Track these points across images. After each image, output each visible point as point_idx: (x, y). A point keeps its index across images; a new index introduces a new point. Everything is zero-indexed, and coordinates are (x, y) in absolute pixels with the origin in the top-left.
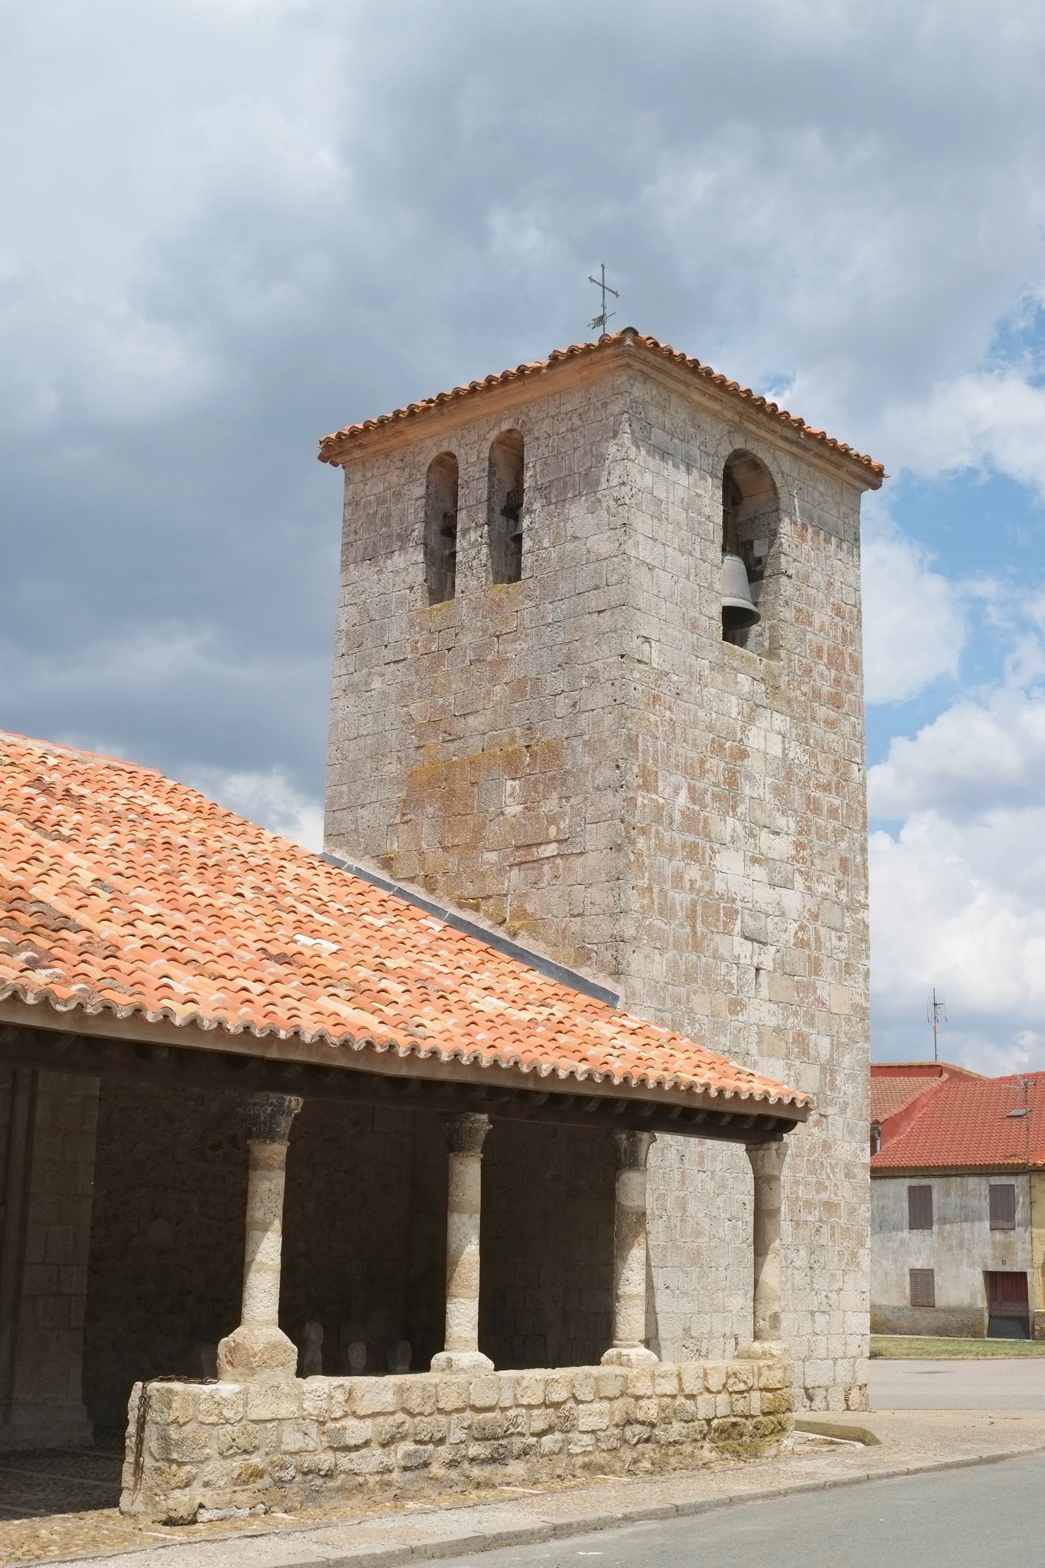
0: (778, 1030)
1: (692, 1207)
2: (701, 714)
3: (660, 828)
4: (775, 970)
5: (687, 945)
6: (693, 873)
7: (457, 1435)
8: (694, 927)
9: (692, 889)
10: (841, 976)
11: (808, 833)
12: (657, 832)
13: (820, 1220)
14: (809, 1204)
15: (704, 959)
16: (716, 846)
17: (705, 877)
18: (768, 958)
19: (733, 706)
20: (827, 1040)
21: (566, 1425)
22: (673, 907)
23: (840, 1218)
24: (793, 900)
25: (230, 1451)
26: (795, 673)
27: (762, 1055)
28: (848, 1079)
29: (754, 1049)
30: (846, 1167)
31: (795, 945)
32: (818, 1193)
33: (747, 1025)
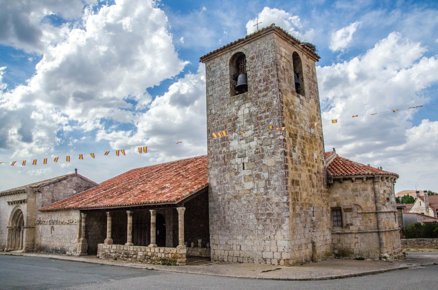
0: (250, 175)
1: (227, 218)
2: (225, 116)
3: (216, 144)
4: (248, 162)
5: (223, 164)
6: (225, 149)
7: (123, 253)
8: (225, 160)
9: (224, 153)
10: (271, 156)
11: (258, 125)
12: (215, 145)
13: (266, 218)
14: (262, 214)
15: (227, 166)
16: (230, 141)
17: (227, 149)
18: (246, 160)
19: (234, 109)
20: (267, 174)
21: (137, 254)
22: (219, 158)
23: (274, 217)
24: (253, 144)
25: (101, 251)
26: (252, 91)
27: (245, 182)
28: (276, 181)
29: (243, 181)
30: (276, 203)
31: (255, 154)
32: (265, 211)
33: (241, 177)
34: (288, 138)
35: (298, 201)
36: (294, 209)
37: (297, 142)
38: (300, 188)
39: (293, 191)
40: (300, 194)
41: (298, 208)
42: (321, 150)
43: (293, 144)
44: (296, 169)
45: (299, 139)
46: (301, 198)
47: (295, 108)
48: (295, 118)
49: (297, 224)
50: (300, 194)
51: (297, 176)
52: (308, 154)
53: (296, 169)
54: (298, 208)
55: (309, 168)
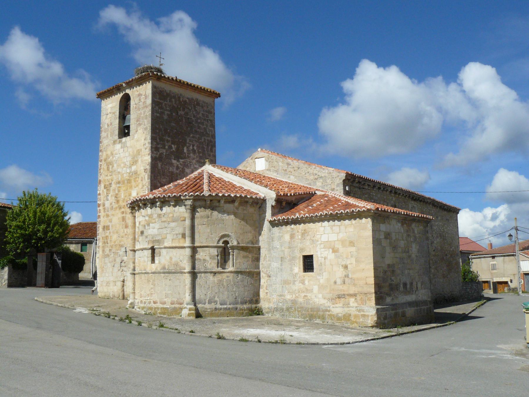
34: (103, 191)
35: (108, 243)
36: (103, 251)
37: (111, 190)
38: (110, 232)
39: (103, 236)
40: (109, 237)
41: (107, 250)
42: (144, 184)
43: (107, 194)
44: (108, 216)
45: (113, 186)
46: (110, 241)
47: (113, 157)
48: (113, 166)
49: (105, 263)
50: (109, 237)
51: (108, 221)
52: (122, 197)
53: (108, 216)
54: (107, 250)
55: (123, 210)
